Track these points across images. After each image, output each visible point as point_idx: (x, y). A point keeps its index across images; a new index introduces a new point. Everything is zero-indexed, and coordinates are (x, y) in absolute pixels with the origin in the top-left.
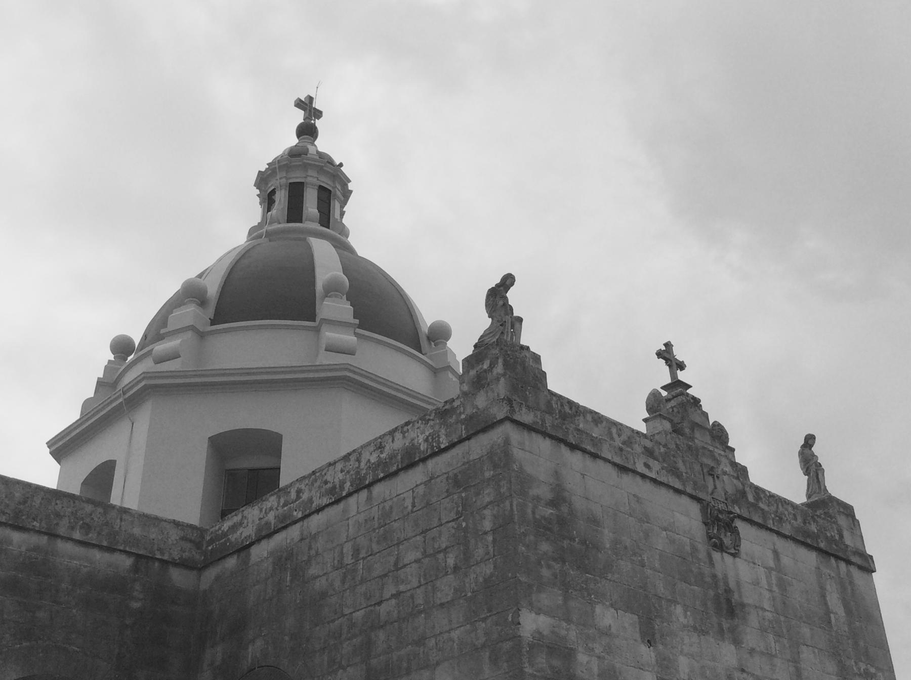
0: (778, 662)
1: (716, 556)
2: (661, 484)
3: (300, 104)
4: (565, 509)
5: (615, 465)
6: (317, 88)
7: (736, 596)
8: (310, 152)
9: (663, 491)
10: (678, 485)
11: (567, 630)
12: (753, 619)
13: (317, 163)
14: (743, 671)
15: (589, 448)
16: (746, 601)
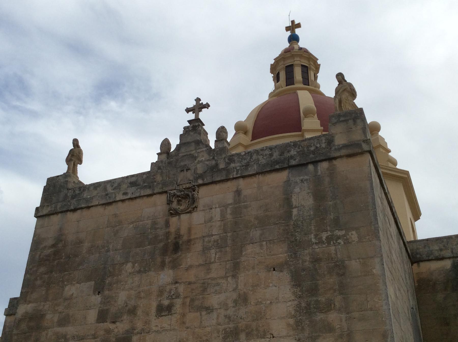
0: (214, 266)
1: (174, 220)
2: (136, 198)
3: (287, 29)
4: (60, 245)
5: (103, 204)
6: (289, 16)
7: (185, 238)
8: (295, 48)
9: (138, 201)
10: (149, 192)
11: (44, 305)
12: (198, 246)
13: (298, 53)
14: (176, 283)
15: (83, 206)
16: (192, 237)
